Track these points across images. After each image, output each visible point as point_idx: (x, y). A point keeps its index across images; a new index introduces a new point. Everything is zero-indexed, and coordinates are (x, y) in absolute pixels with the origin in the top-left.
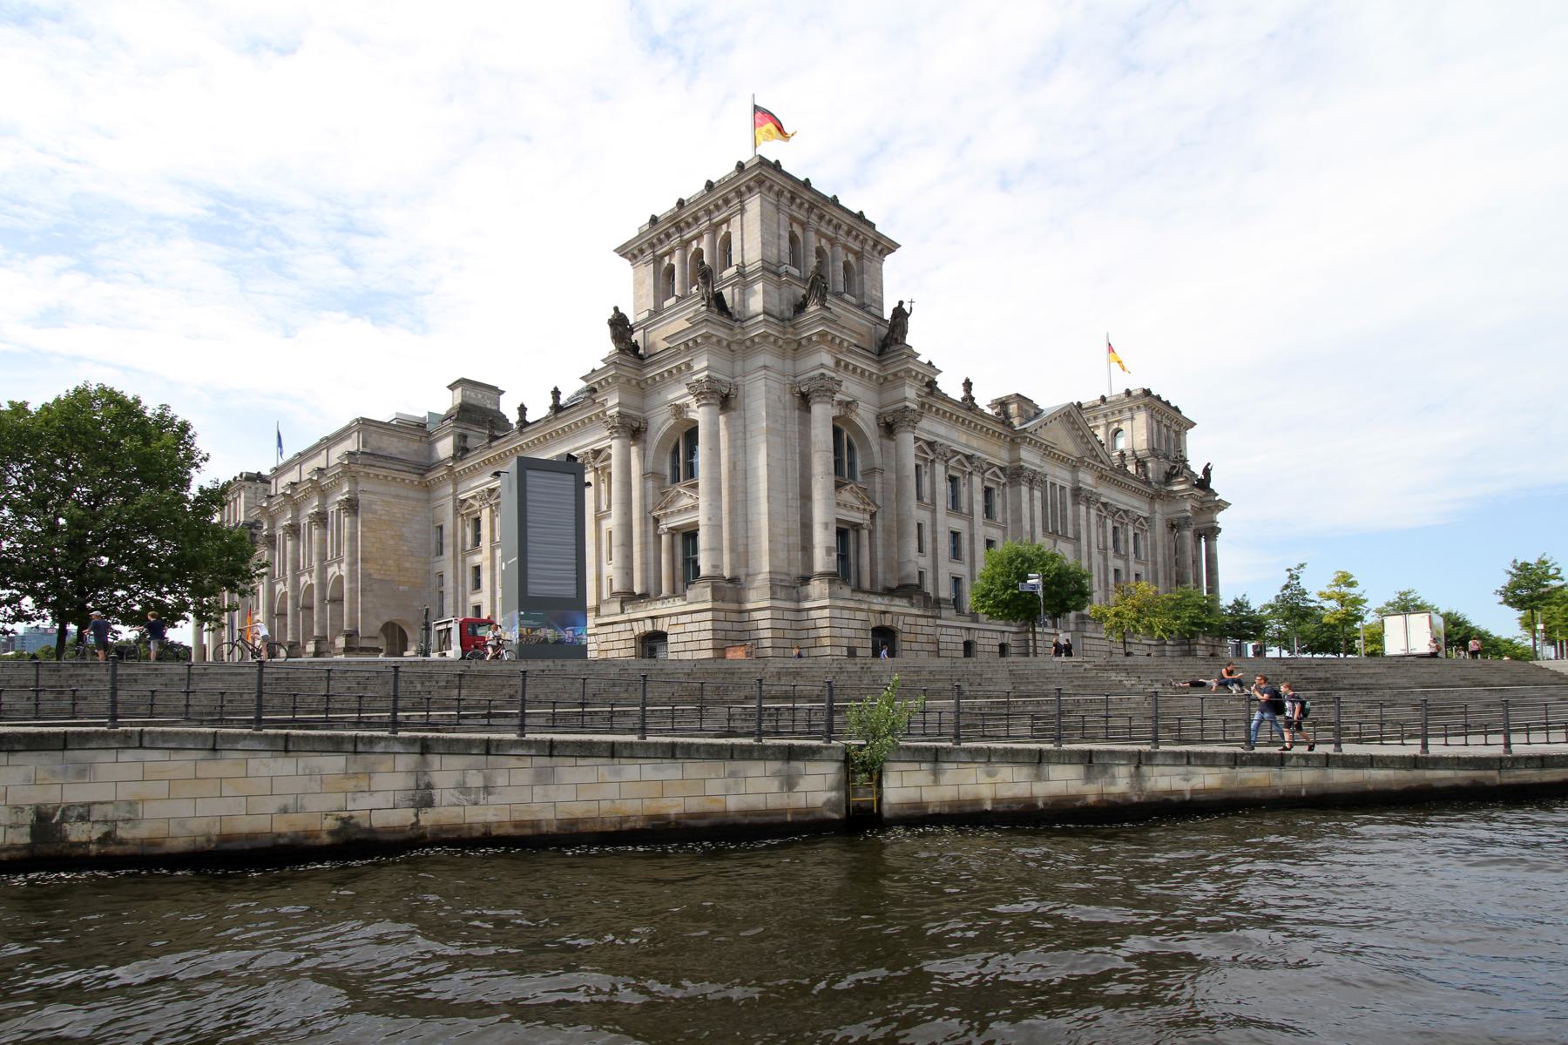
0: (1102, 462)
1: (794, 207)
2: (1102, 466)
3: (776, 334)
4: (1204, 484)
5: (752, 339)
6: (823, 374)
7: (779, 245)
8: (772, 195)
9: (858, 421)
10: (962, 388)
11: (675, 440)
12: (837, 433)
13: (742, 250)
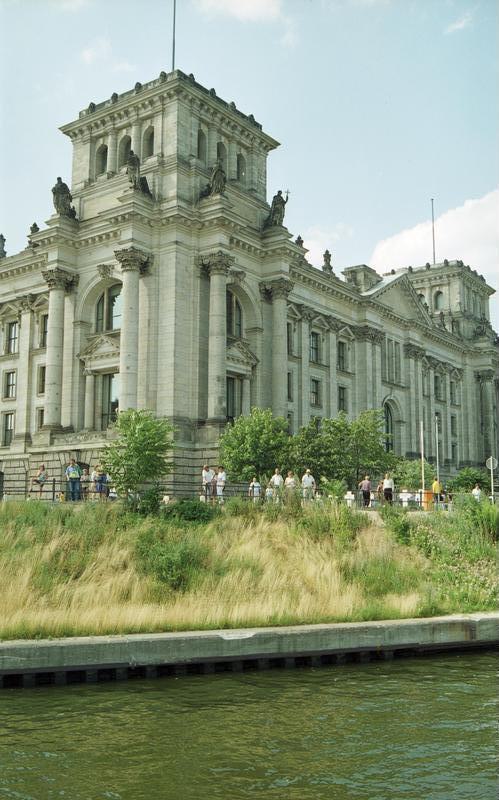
1: (202, 112)
5: (167, 219)
6: (220, 251)
8: (186, 101)
9: (245, 288)
10: (323, 259)
11: (101, 294)
12: (229, 295)
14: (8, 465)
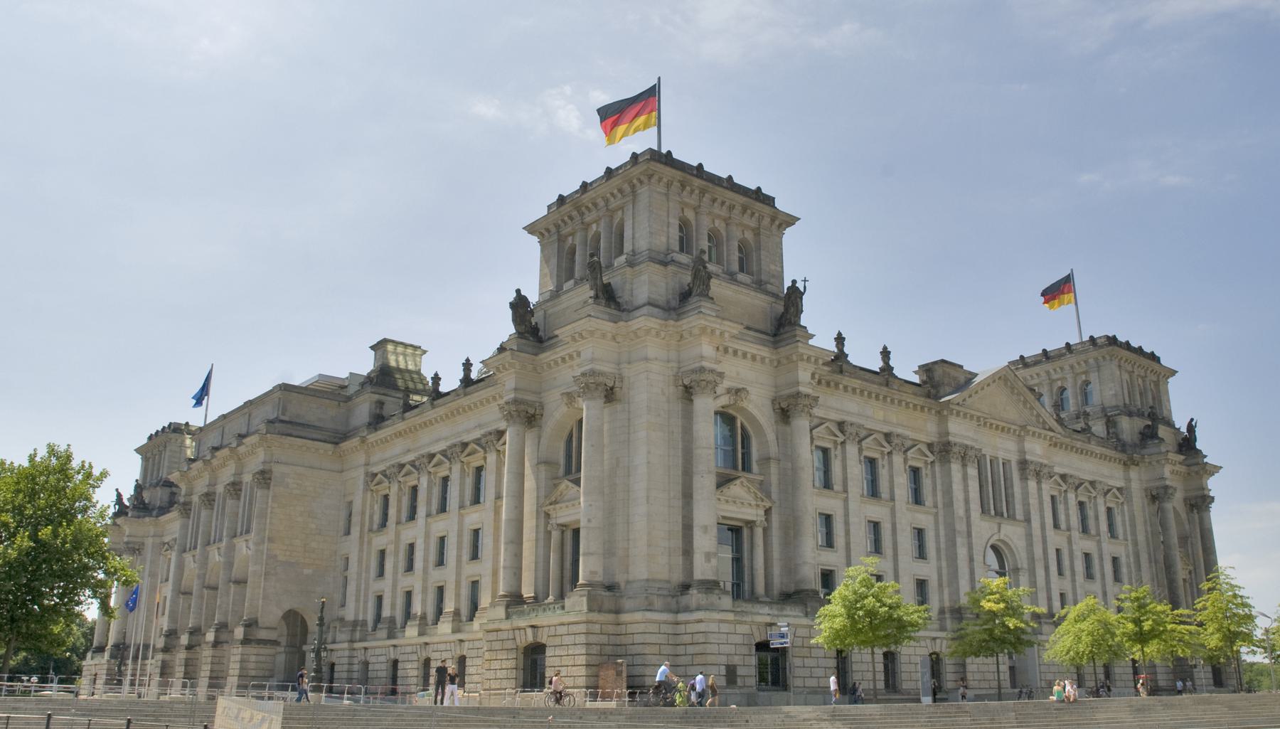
0: (1053, 431)
2: (1052, 434)
3: (657, 327)
4: (1187, 444)
5: (635, 333)
7: (668, 232)
9: (751, 408)
13: (633, 238)
14: (471, 646)
